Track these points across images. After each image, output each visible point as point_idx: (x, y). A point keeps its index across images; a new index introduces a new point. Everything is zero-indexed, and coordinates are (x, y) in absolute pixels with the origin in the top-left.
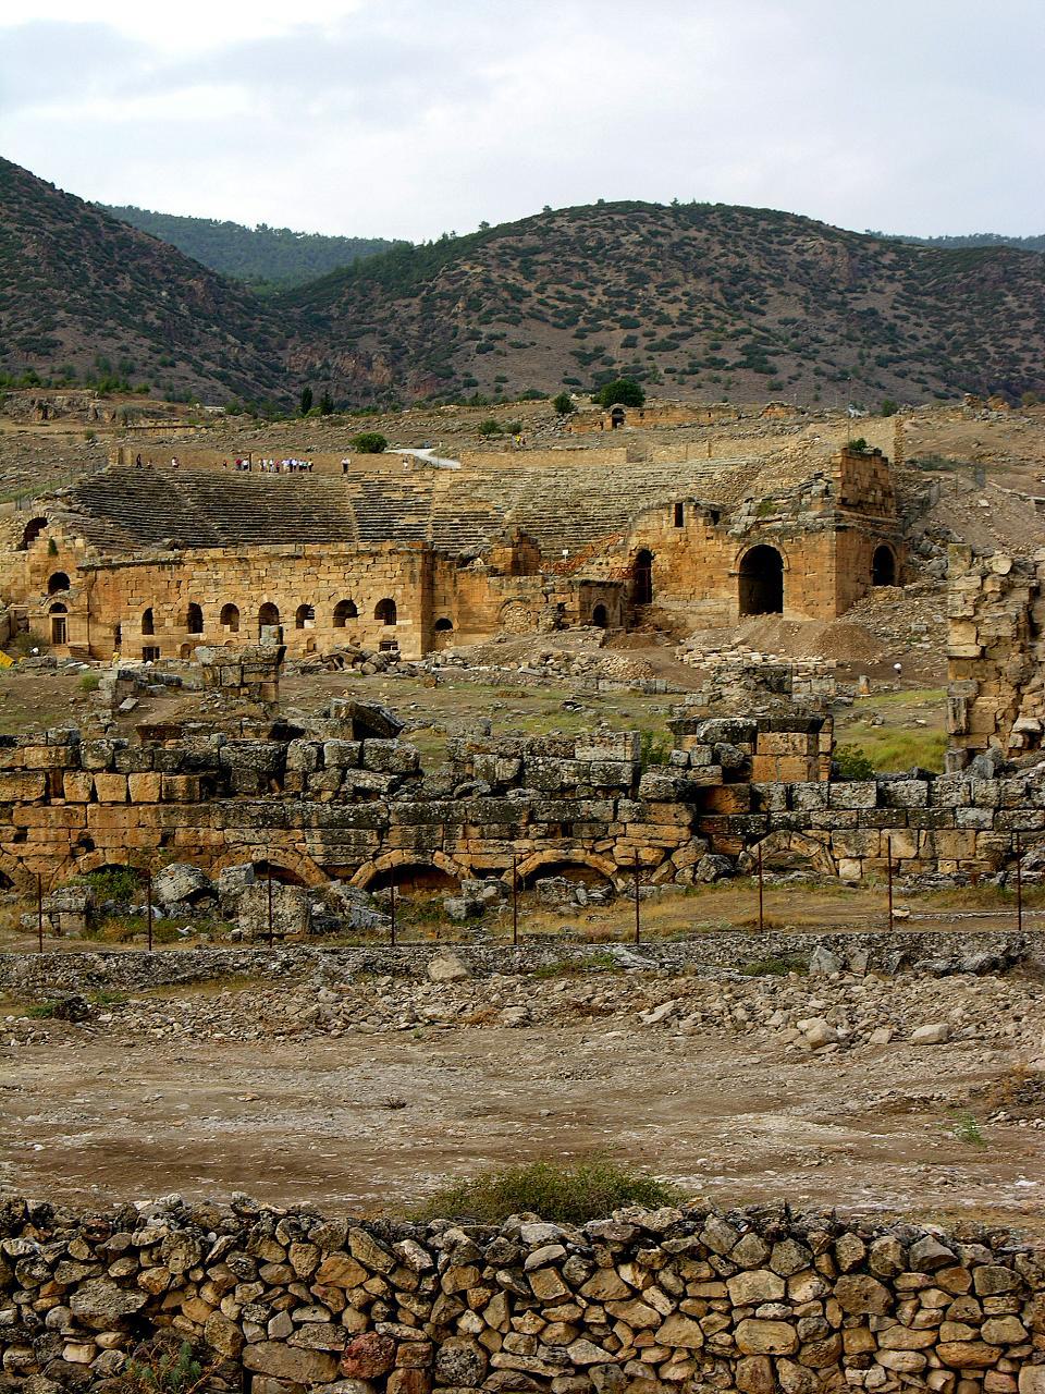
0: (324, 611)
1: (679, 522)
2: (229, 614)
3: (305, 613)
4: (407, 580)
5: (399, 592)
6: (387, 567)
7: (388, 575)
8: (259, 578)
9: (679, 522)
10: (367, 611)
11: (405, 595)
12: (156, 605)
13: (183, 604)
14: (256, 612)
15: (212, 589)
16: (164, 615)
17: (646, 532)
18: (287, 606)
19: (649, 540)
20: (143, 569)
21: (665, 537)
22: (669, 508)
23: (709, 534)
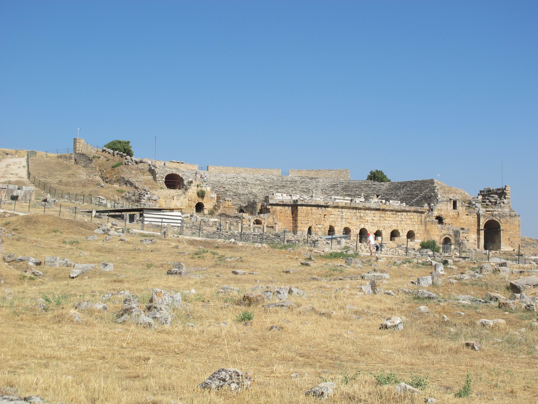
0: (386, 234)
1: (455, 207)
2: (347, 231)
3: (378, 234)
4: (419, 223)
5: (416, 228)
6: (412, 217)
7: (413, 220)
8: (361, 217)
9: (455, 207)
10: (403, 235)
11: (418, 229)
12: (314, 225)
13: (327, 225)
14: (358, 232)
15: (340, 220)
16: (318, 230)
17: (441, 210)
18: (372, 230)
19: (442, 213)
20: (309, 208)
21: (449, 213)
22: (451, 202)
23: (467, 213)
